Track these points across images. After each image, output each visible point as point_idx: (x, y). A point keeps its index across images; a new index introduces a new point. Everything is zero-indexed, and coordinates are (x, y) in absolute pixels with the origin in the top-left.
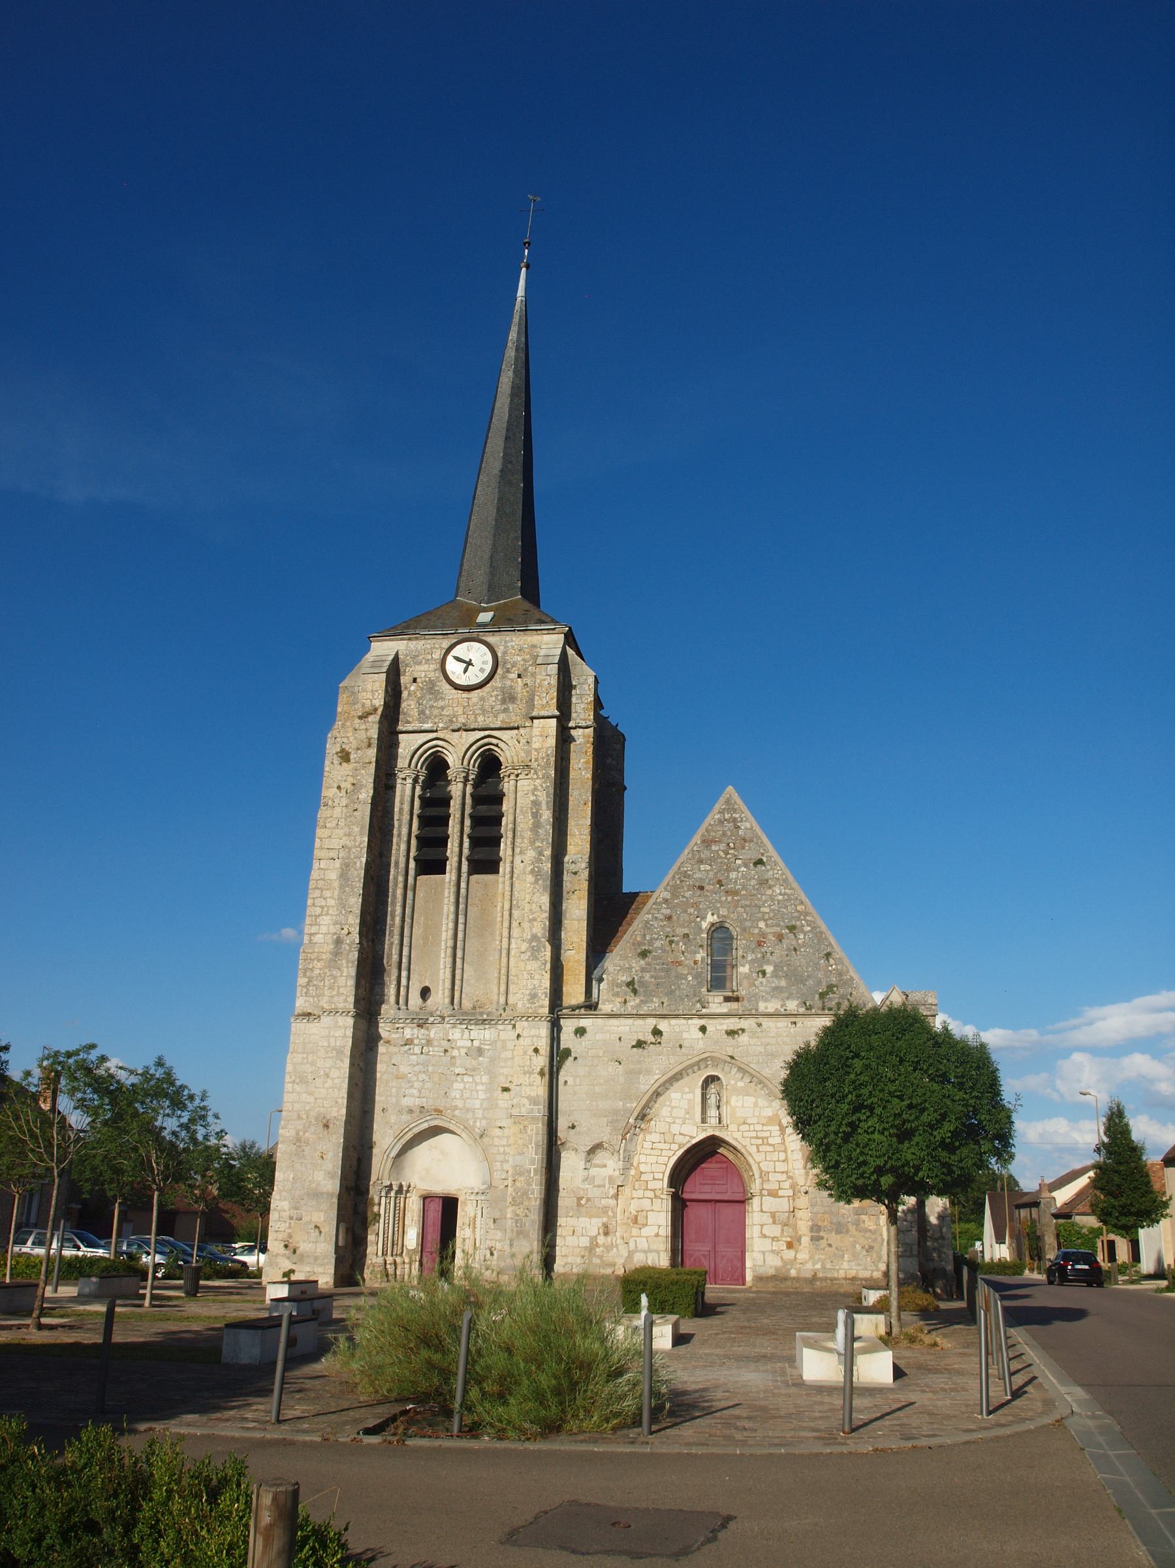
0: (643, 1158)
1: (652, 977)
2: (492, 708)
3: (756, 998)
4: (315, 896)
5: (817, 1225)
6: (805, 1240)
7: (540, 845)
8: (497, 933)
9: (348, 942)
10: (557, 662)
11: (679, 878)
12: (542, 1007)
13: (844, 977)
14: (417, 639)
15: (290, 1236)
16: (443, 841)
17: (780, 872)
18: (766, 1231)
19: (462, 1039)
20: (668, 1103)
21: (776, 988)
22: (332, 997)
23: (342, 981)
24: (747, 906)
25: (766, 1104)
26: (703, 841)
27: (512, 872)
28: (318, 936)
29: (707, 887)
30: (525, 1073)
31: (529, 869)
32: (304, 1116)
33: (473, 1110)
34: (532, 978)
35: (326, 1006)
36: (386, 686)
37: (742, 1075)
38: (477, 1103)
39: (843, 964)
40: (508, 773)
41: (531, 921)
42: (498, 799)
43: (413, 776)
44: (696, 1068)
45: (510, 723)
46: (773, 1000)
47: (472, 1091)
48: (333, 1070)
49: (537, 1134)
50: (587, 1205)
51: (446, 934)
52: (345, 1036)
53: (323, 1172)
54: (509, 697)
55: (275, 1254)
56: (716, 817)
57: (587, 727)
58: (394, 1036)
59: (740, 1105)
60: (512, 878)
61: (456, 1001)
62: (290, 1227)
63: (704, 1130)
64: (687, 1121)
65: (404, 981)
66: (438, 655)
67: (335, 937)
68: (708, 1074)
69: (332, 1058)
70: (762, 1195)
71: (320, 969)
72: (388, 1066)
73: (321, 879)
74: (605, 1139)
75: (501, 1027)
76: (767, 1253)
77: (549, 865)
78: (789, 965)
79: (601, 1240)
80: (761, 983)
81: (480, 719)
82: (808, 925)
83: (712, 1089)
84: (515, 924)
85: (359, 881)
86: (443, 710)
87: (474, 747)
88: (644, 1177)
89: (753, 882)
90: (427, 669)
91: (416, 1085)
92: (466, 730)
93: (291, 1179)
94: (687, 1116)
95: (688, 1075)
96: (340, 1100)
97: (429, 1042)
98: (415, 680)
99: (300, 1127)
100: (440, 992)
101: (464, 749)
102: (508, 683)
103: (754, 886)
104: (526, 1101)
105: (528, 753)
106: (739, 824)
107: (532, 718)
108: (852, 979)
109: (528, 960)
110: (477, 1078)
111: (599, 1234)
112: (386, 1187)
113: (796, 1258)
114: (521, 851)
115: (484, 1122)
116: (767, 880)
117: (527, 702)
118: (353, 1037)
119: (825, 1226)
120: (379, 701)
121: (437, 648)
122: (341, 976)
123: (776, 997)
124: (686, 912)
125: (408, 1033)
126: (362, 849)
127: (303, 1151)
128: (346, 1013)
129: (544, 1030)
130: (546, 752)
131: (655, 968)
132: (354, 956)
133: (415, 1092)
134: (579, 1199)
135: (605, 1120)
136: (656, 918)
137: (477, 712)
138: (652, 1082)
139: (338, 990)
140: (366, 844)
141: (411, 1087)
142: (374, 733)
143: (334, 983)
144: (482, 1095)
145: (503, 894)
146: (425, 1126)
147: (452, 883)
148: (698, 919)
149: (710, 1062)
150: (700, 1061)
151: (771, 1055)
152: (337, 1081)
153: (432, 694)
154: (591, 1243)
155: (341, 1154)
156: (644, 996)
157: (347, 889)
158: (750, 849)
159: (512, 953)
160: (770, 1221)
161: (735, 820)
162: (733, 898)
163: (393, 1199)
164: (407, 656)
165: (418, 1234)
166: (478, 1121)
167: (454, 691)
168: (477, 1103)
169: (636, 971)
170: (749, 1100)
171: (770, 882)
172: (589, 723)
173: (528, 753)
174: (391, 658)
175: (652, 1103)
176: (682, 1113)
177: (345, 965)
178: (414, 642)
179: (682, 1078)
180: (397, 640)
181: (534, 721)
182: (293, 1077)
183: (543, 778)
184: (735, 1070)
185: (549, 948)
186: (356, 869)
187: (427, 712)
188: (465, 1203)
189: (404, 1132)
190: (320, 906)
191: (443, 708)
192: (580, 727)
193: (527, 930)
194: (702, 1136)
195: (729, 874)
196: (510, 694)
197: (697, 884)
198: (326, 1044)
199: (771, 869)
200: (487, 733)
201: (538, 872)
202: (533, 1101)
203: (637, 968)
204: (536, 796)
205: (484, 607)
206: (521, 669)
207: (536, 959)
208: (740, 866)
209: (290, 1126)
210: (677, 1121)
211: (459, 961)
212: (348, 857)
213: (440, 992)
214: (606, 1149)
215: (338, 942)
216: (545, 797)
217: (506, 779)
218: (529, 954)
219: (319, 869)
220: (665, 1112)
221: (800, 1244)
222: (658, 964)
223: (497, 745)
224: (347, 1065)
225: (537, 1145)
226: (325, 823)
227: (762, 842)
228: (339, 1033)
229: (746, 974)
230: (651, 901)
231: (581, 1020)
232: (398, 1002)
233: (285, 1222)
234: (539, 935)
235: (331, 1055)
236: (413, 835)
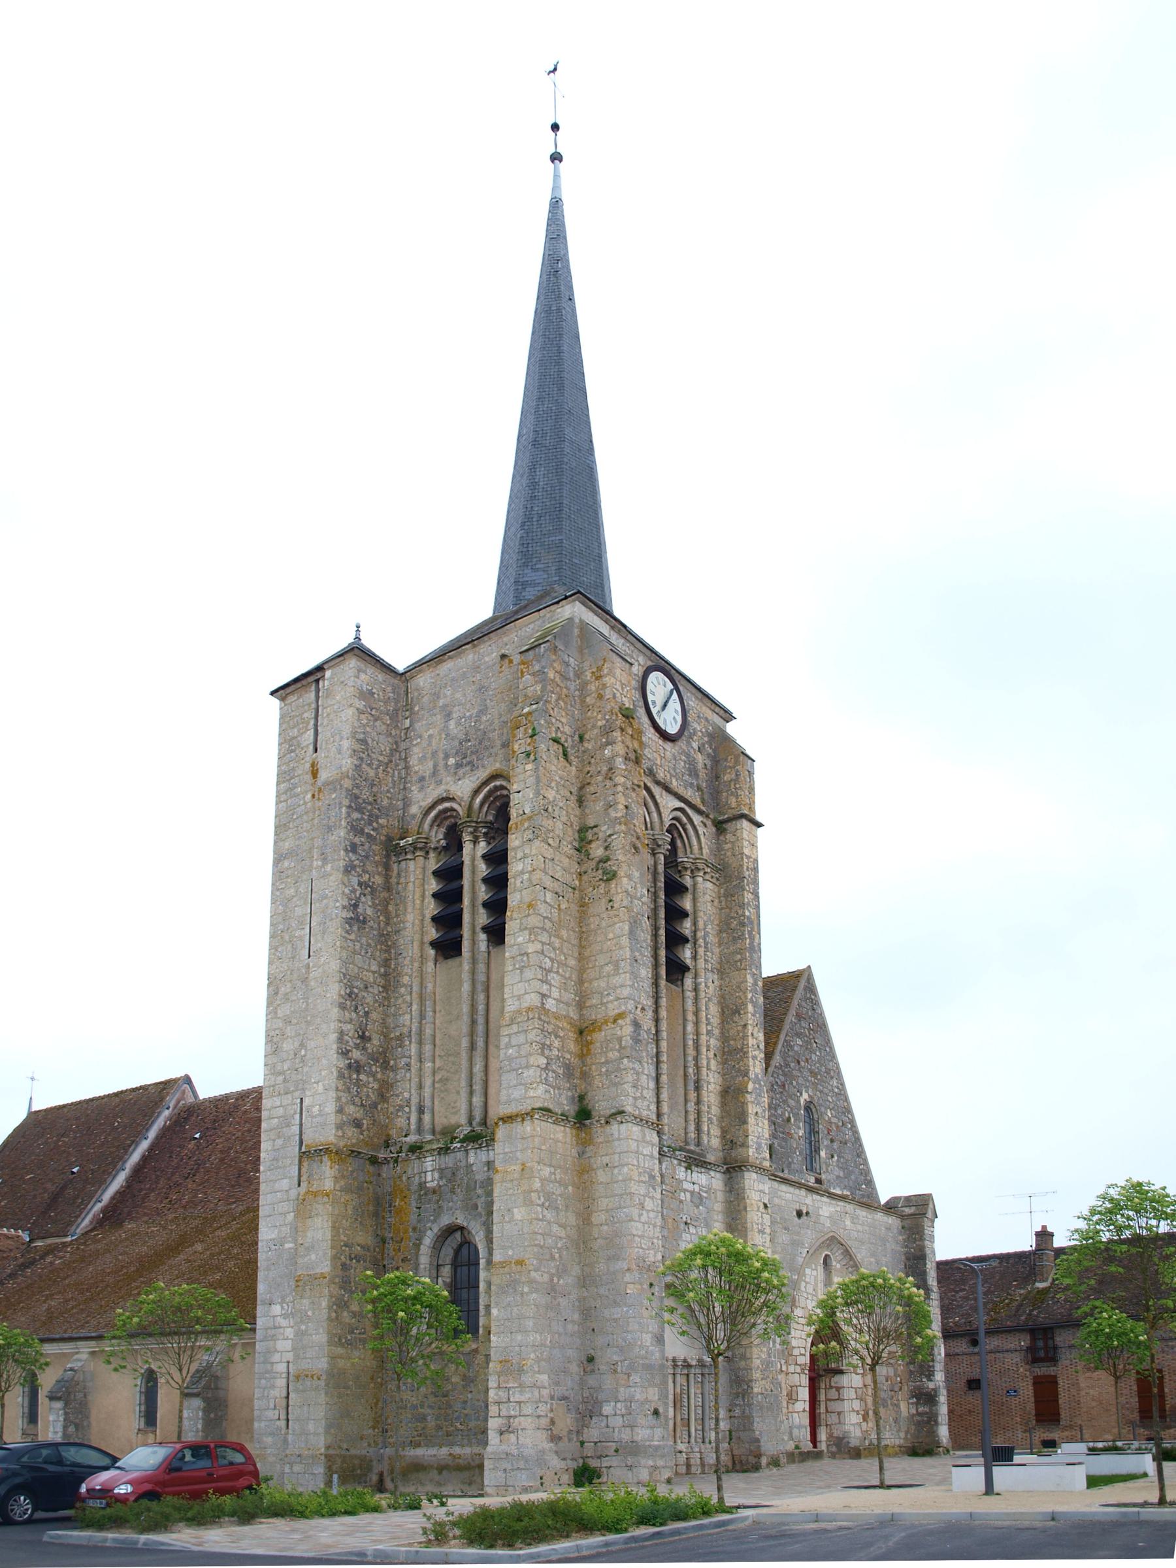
22: (635, 1099)
28: (550, 1000)
29: (802, 1064)
32: (557, 1256)
34: (758, 1125)
71: (559, 1050)
89: (823, 1069)
96: (655, 1241)
171: (832, 1074)
182: (542, 1199)
235: (644, 1179)
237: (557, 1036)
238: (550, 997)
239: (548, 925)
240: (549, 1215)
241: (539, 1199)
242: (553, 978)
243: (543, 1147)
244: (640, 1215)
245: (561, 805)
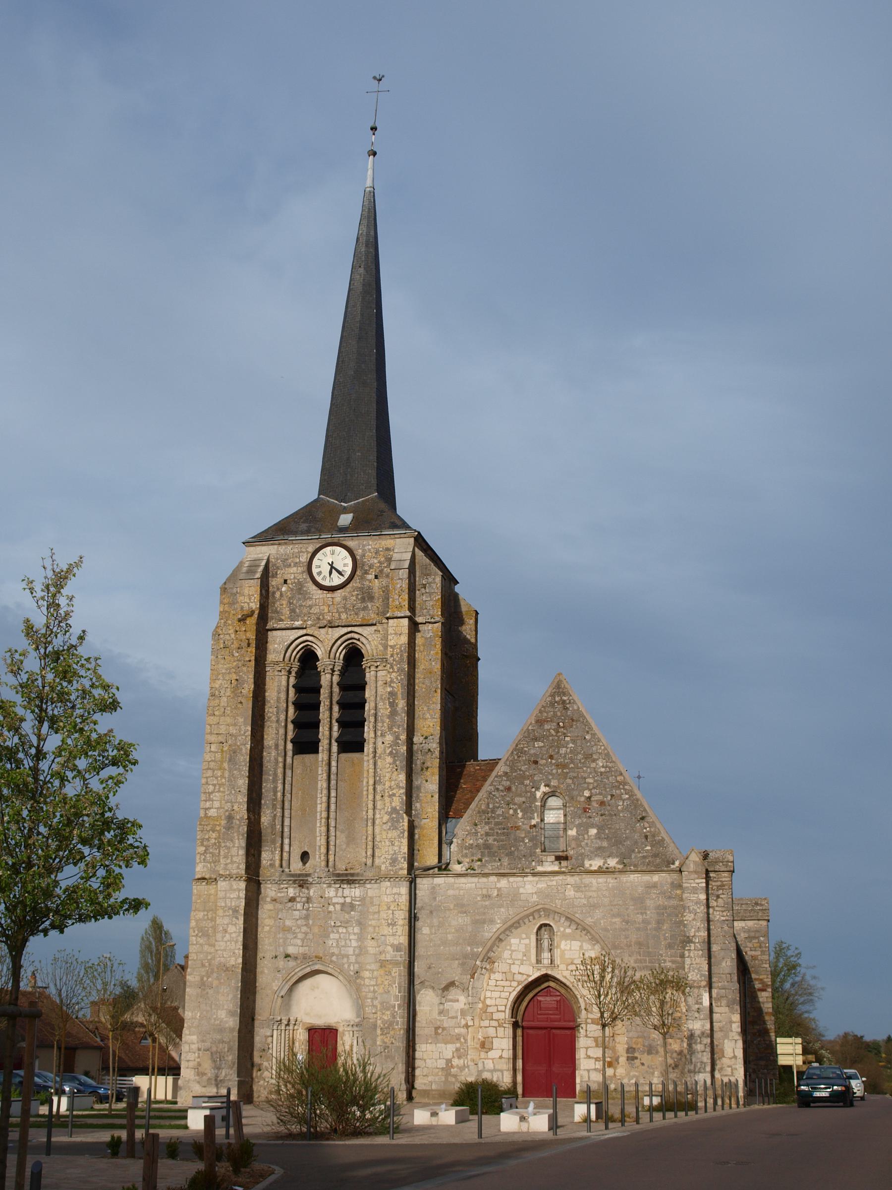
0: (488, 994)
1: (495, 840)
2: (354, 607)
3: (582, 857)
4: (208, 775)
5: (632, 1048)
6: (623, 1060)
7: (397, 730)
8: (364, 805)
9: (238, 817)
10: (407, 567)
11: (517, 754)
12: (401, 869)
13: (657, 838)
14: (286, 543)
15: (199, 1064)
16: (316, 725)
17: (603, 748)
18: (591, 1052)
19: (336, 896)
20: (508, 947)
21: (599, 848)
22: (226, 864)
23: (234, 851)
24: (575, 777)
25: (590, 947)
26: (537, 721)
27: (375, 752)
28: (212, 810)
30: (389, 925)
31: (388, 751)
32: (207, 964)
33: (347, 956)
34: (393, 845)
35: (221, 872)
36: (261, 591)
37: (569, 923)
38: (350, 951)
39: (656, 827)
40: (369, 665)
41: (390, 796)
42: (361, 687)
43: (288, 669)
44: (531, 918)
45: (369, 620)
46: (596, 859)
47: (346, 940)
48: (230, 926)
49: (400, 975)
50: (444, 1034)
51: (321, 807)
52: (239, 898)
53: (225, 1011)
54: (367, 596)
55: (187, 1079)
56: (548, 699)
57: (435, 623)
58: (279, 895)
59: (568, 949)
60: (375, 757)
61: (331, 864)
62: (199, 1057)
63: (538, 970)
64: (525, 962)
65: (286, 848)
66: (304, 558)
67: (227, 814)
68: (542, 923)
69: (228, 916)
70: (587, 1023)
71: (215, 839)
72: (275, 921)
73: (212, 761)
74: (457, 978)
75: (368, 886)
76: (591, 1072)
77: (405, 748)
78: (610, 828)
79: (456, 1062)
80: (587, 844)
81: (344, 616)
82: (626, 794)
83: (545, 935)
84: (378, 797)
85: (246, 765)
86: (311, 609)
87: (339, 642)
88: (490, 1010)
89: (580, 756)
90: (295, 571)
91: (300, 936)
92: (330, 627)
93: (198, 1017)
94: (525, 958)
95: (525, 924)
96: (237, 951)
97: (309, 900)
98: (285, 582)
99: (204, 974)
100: (317, 856)
101: (331, 644)
102: (367, 583)
103: (580, 760)
104: (389, 948)
105: (386, 647)
106: (568, 706)
107: (388, 618)
108: (663, 840)
109: (389, 829)
110: (350, 929)
111: (453, 1057)
113: (615, 1074)
114: (381, 734)
115: (357, 966)
116: (591, 755)
117: (383, 601)
118: (246, 898)
119: (639, 1048)
120: (255, 605)
121: (304, 552)
122: (234, 846)
123: (599, 856)
124: (523, 783)
125: (291, 892)
126: (246, 736)
127: (207, 993)
128: (238, 878)
129: (404, 890)
130: (400, 648)
131: (497, 833)
132: (243, 829)
133: (299, 942)
134: (437, 1028)
135: (457, 962)
136: (498, 789)
137: (341, 610)
138: (494, 930)
139: (232, 858)
140: (250, 733)
141: (295, 937)
142: (252, 636)
143: (228, 853)
144: (354, 944)
145: (368, 771)
146: (308, 970)
147: (324, 763)
148: (533, 790)
149: (542, 913)
150: (534, 912)
151: (593, 906)
152: (234, 935)
153: (301, 594)
154: (447, 1064)
155: (239, 996)
156: (488, 856)
157: (235, 772)
158: (577, 727)
159: (377, 822)
160: (594, 1044)
161: (564, 702)
162: (562, 771)
163: (283, 1031)
164: (277, 559)
167: (320, 592)
168: (350, 951)
169: (481, 835)
170: (576, 945)
171: (595, 757)
172: (437, 619)
173: (386, 647)
174: (263, 563)
175: (496, 947)
176: (520, 956)
177: (236, 838)
178: (284, 547)
179: (520, 926)
180: (268, 545)
181: (390, 620)
182: (196, 932)
183: (398, 671)
184: (563, 919)
185: (406, 818)
186: (242, 755)
187: (297, 611)
189: (291, 975)
190: (213, 785)
191: (310, 607)
192: (430, 623)
193: (388, 804)
194: (537, 974)
195: (559, 750)
196: (368, 592)
197: (532, 759)
198: (223, 904)
199: (595, 745)
200: (350, 629)
201: (396, 753)
202: (397, 948)
203: (482, 833)
204: (393, 687)
205: (345, 507)
206: (378, 570)
207: (396, 828)
208: (568, 743)
209: (195, 973)
210: (517, 962)
211: (332, 829)
212: (235, 744)
213: (317, 856)
214: (458, 986)
215: (230, 818)
216: (399, 689)
217: (367, 670)
218: (389, 824)
219: (210, 752)
220: (506, 954)
221: (618, 1063)
222: (500, 829)
223: (359, 640)
224: (242, 922)
225: (400, 987)
226: (214, 711)
227: (587, 721)
228: (234, 895)
229: (573, 836)
230: (494, 774)
231: (435, 879)
232: (281, 866)
233: (195, 1053)
234: (398, 808)
236: (289, 720)
237: (213, 832)
238: (210, 808)
239: (212, 765)
240: (201, 941)
241: (194, 932)
242: (215, 796)
243: (199, 901)
244: (223, 937)
245: (226, 686)
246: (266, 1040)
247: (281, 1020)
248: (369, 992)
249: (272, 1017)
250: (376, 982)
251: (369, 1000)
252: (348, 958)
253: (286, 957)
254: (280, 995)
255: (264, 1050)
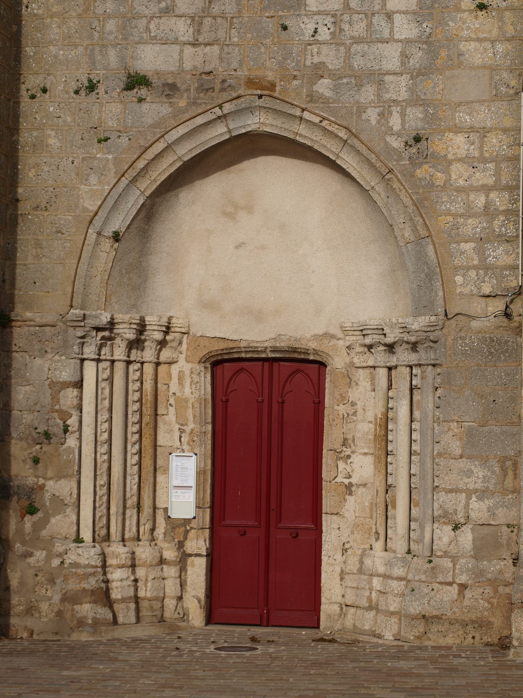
47: (369, 15)
112: (98, 329)
163: (119, 367)
165: (200, 473)
166: (395, 110)
188: (350, 381)
189: (150, 155)
246: (55, 399)
247: (112, 324)
248: (467, 215)
249: (76, 312)
250: (497, 174)
251: (468, 247)
252: (381, 83)
253: (129, 87)
254: (109, 231)
255: (47, 435)
